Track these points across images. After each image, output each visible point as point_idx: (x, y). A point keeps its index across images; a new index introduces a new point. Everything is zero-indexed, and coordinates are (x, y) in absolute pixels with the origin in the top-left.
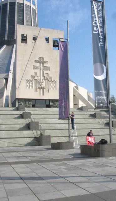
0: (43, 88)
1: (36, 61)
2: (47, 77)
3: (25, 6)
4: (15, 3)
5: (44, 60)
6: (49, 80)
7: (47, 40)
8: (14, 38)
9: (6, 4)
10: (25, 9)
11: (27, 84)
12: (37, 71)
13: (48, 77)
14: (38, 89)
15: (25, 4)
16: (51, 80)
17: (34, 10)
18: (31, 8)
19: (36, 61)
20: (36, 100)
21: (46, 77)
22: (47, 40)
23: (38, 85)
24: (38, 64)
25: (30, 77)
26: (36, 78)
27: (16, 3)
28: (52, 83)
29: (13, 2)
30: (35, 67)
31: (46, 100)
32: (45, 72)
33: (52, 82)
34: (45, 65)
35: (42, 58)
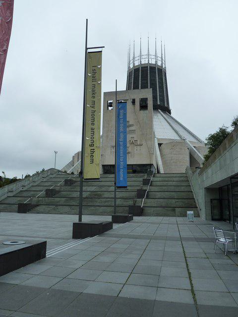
3: (149, 69)
7: (134, 102)
22: (134, 102)
28: (138, 147)
31: (132, 165)
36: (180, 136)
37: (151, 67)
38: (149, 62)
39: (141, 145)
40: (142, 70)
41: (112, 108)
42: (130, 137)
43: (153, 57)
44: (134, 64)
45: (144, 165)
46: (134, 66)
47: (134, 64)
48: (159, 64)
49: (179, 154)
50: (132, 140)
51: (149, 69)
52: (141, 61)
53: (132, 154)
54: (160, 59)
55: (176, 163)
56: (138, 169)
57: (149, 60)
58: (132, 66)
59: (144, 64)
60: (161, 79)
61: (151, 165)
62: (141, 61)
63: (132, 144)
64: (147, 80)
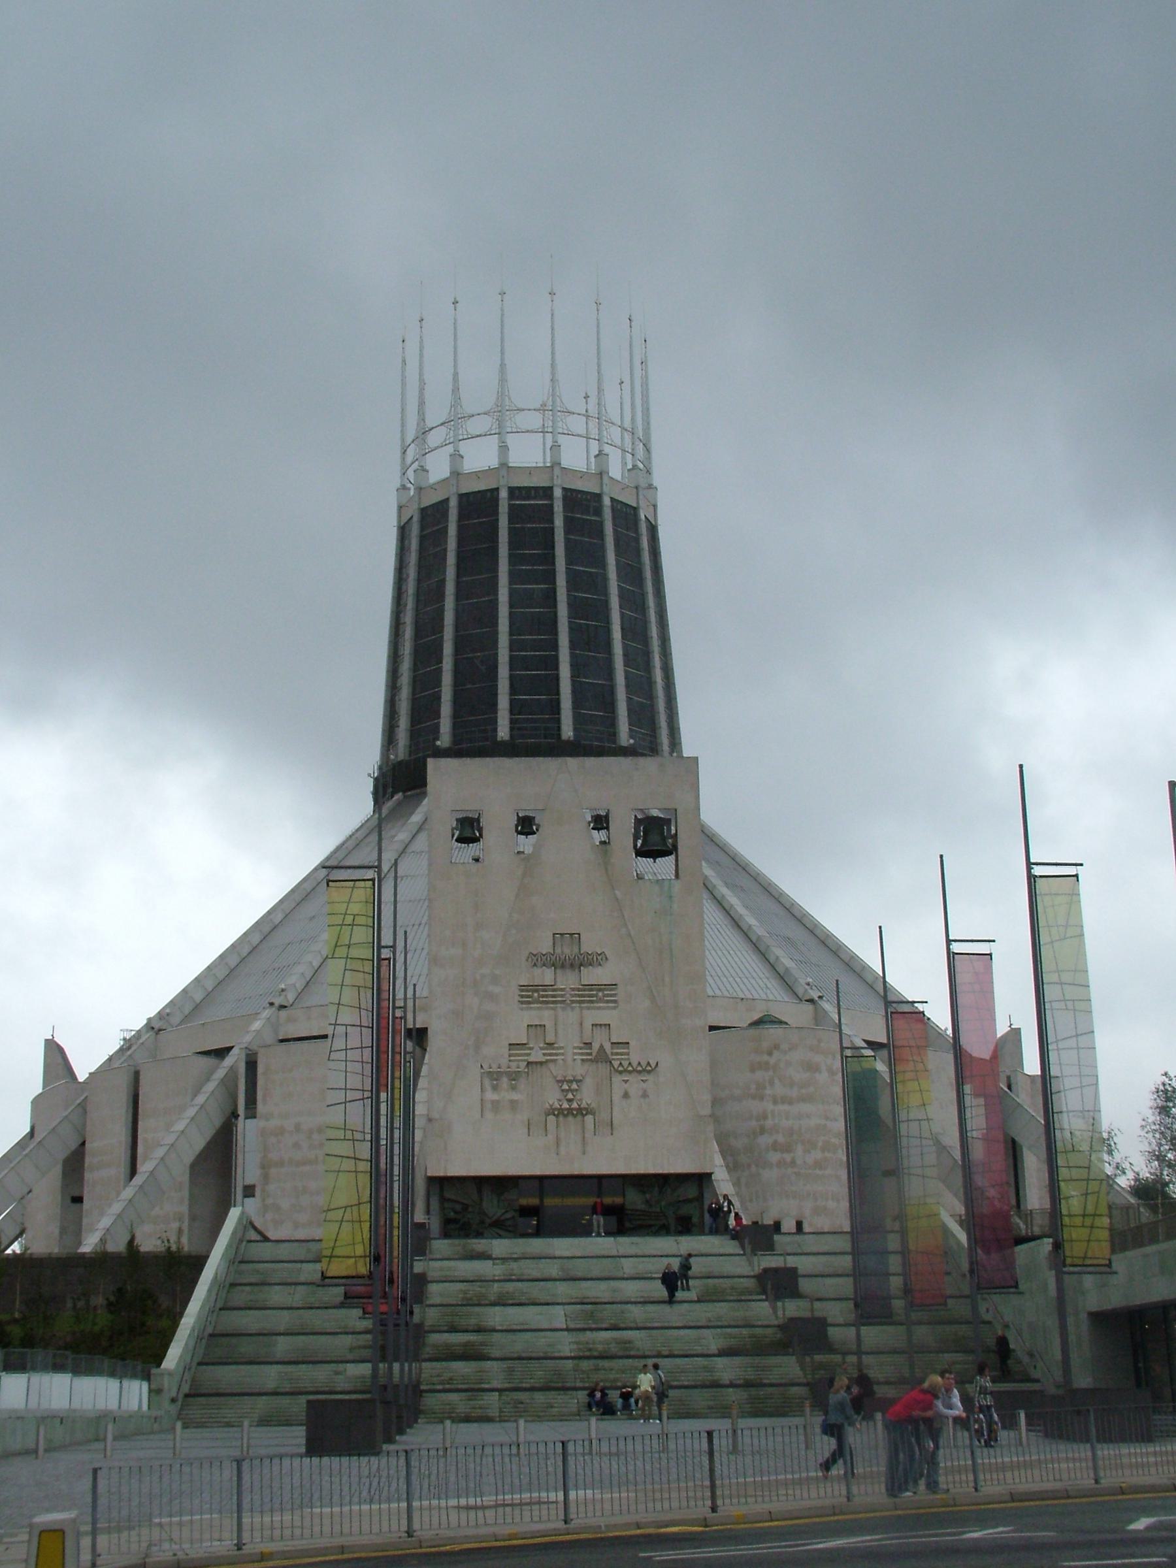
0: (582, 1112)
1: (538, 960)
2: (602, 1046)
3: (558, 507)
4: (497, 489)
5: (589, 946)
6: (616, 1063)
8: (495, 730)
9: (441, 508)
10: (559, 522)
11: (490, 1095)
12: (545, 1016)
13: (607, 1047)
14: (551, 1118)
15: (558, 493)
16: (625, 1064)
17: (627, 516)
18: (607, 501)
19: (538, 960)
20: (541, 1179)
21: (596, 1046)
23: (553, 1097)
24: (547, 976)
25: (505, 1051)
26: (538, 1055)
27: (504, 494)
29: (483, 488)
30: (532, 994)
32: (592, 1016)
33: (634, 1070)
34: (592, 976)
35: (575, 937)
36: (784, 979)
37: (573, 498)
38: (556, 464)
39: (648, 1070)
40: (511, 508)
41: (472, 849)
42: (588, 1025)
43: (577, 424)
44: (457, 457)
45: (663, 1180)
46: (456, 474)
47: (457, 457)
48: (615, 471)
49: (803, 1099)
50: (600, 1040)
51: (558, 507)
52: (504, 449)
53: (604, 1115)
54: (615, 433)
55: (787, 1148)
56: (634, 1199)
57: (556, 447)
58: (438, 469)
59: (530, 471)
60: (632, 574)
61: (702, 1179)
62: (504, 449)
63: (595, 1061)
64: (550, 577)
